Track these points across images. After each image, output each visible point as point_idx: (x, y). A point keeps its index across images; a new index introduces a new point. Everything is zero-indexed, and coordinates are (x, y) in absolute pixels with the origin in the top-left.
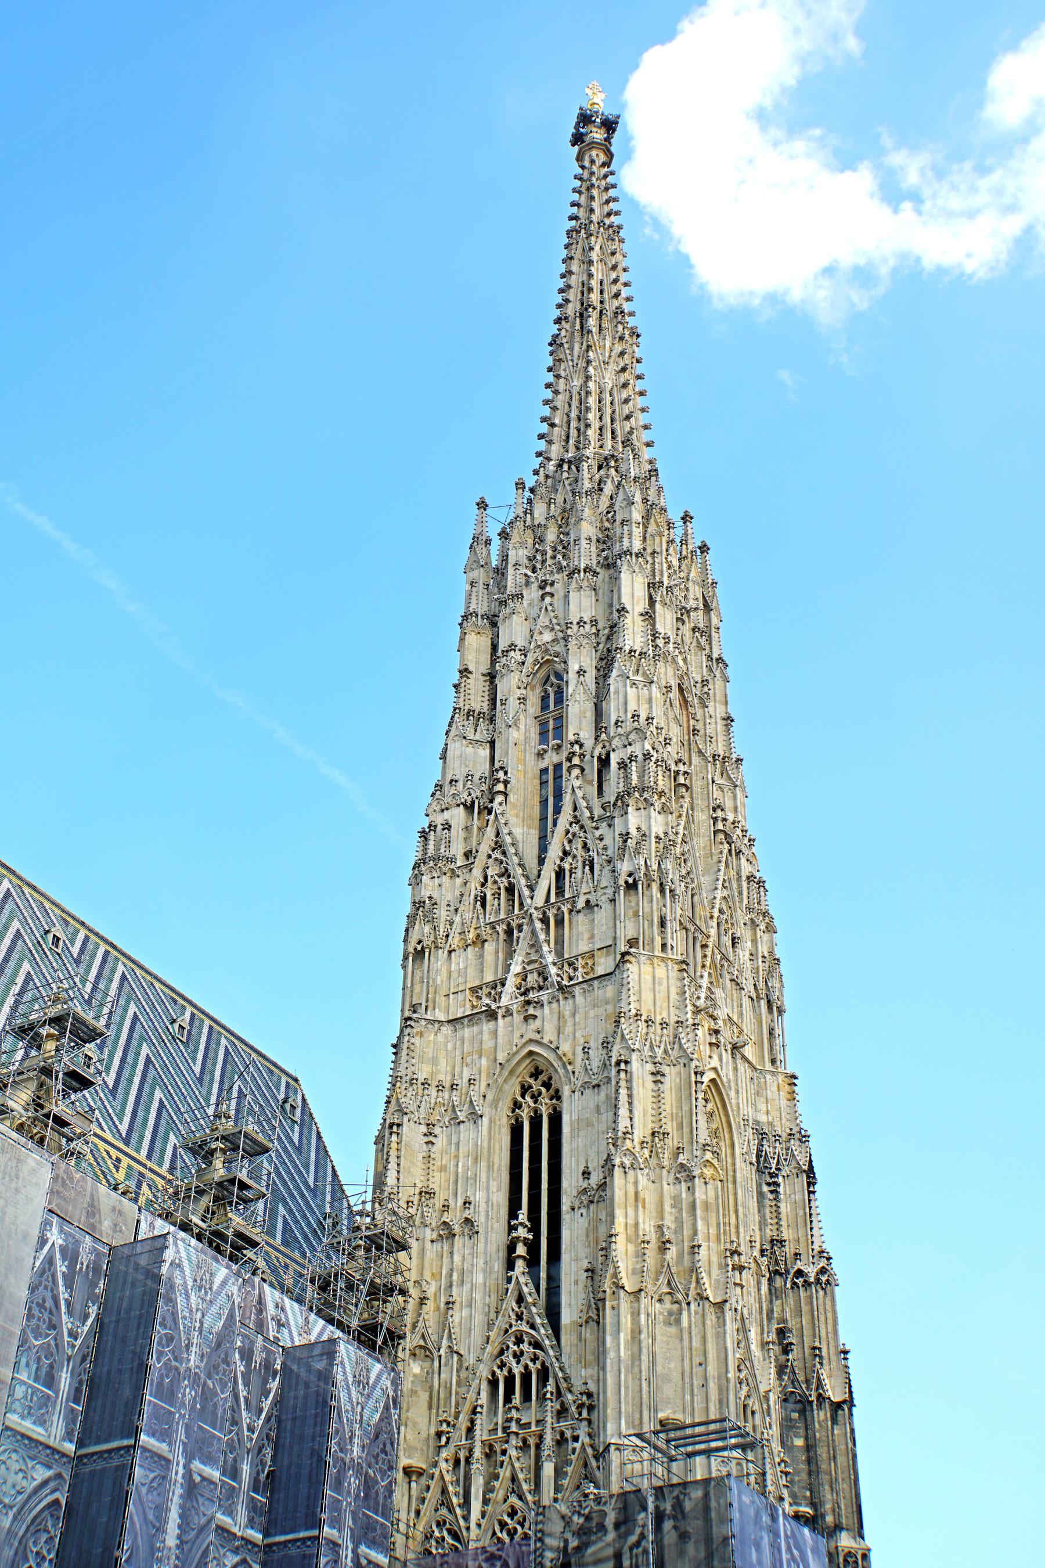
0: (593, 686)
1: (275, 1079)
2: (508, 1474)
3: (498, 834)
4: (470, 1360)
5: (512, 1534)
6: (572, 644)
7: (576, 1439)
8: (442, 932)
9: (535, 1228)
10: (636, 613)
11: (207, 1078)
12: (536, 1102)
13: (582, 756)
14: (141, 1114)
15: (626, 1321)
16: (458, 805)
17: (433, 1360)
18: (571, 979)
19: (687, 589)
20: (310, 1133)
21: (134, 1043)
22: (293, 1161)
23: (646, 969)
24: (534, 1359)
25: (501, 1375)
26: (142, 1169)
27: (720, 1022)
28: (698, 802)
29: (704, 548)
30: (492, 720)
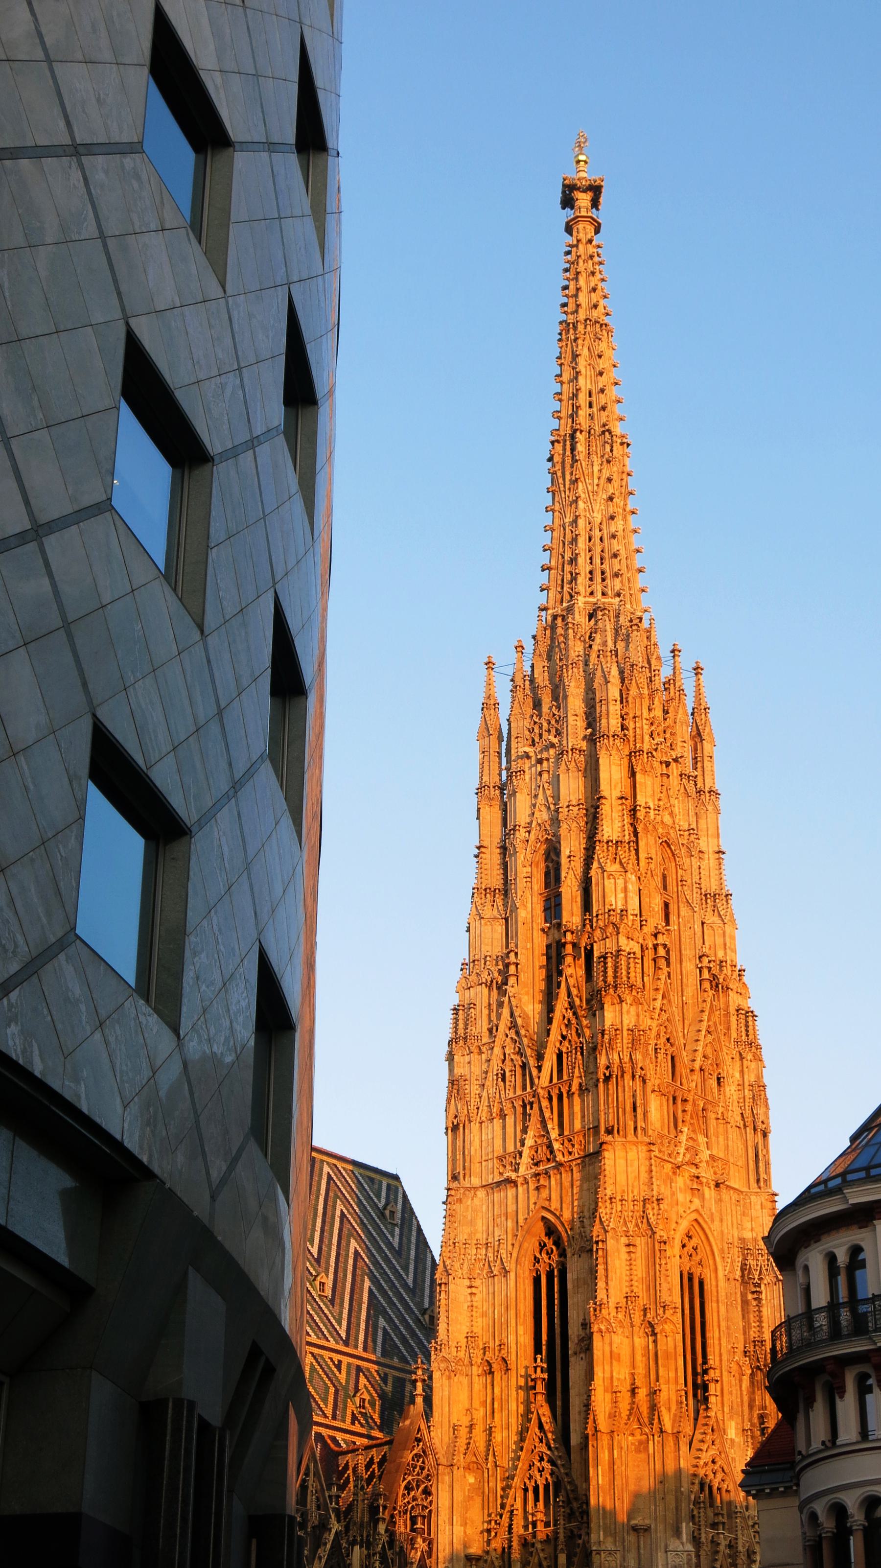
1: (376, 1186)
2: (536, 1560)
3: (512, 1014)
6: (563, 831)
8: (472, 1108)
10: (614, 798)
15: (604, 1456)
16: (481, 984)
18: (570, 1153)
20: (410, 1230)
23: (620, 1153)
25: (531, 1485)
27: (703, 1165)
28: (688, 952)
29: (698, 670)
30: (506, 893)
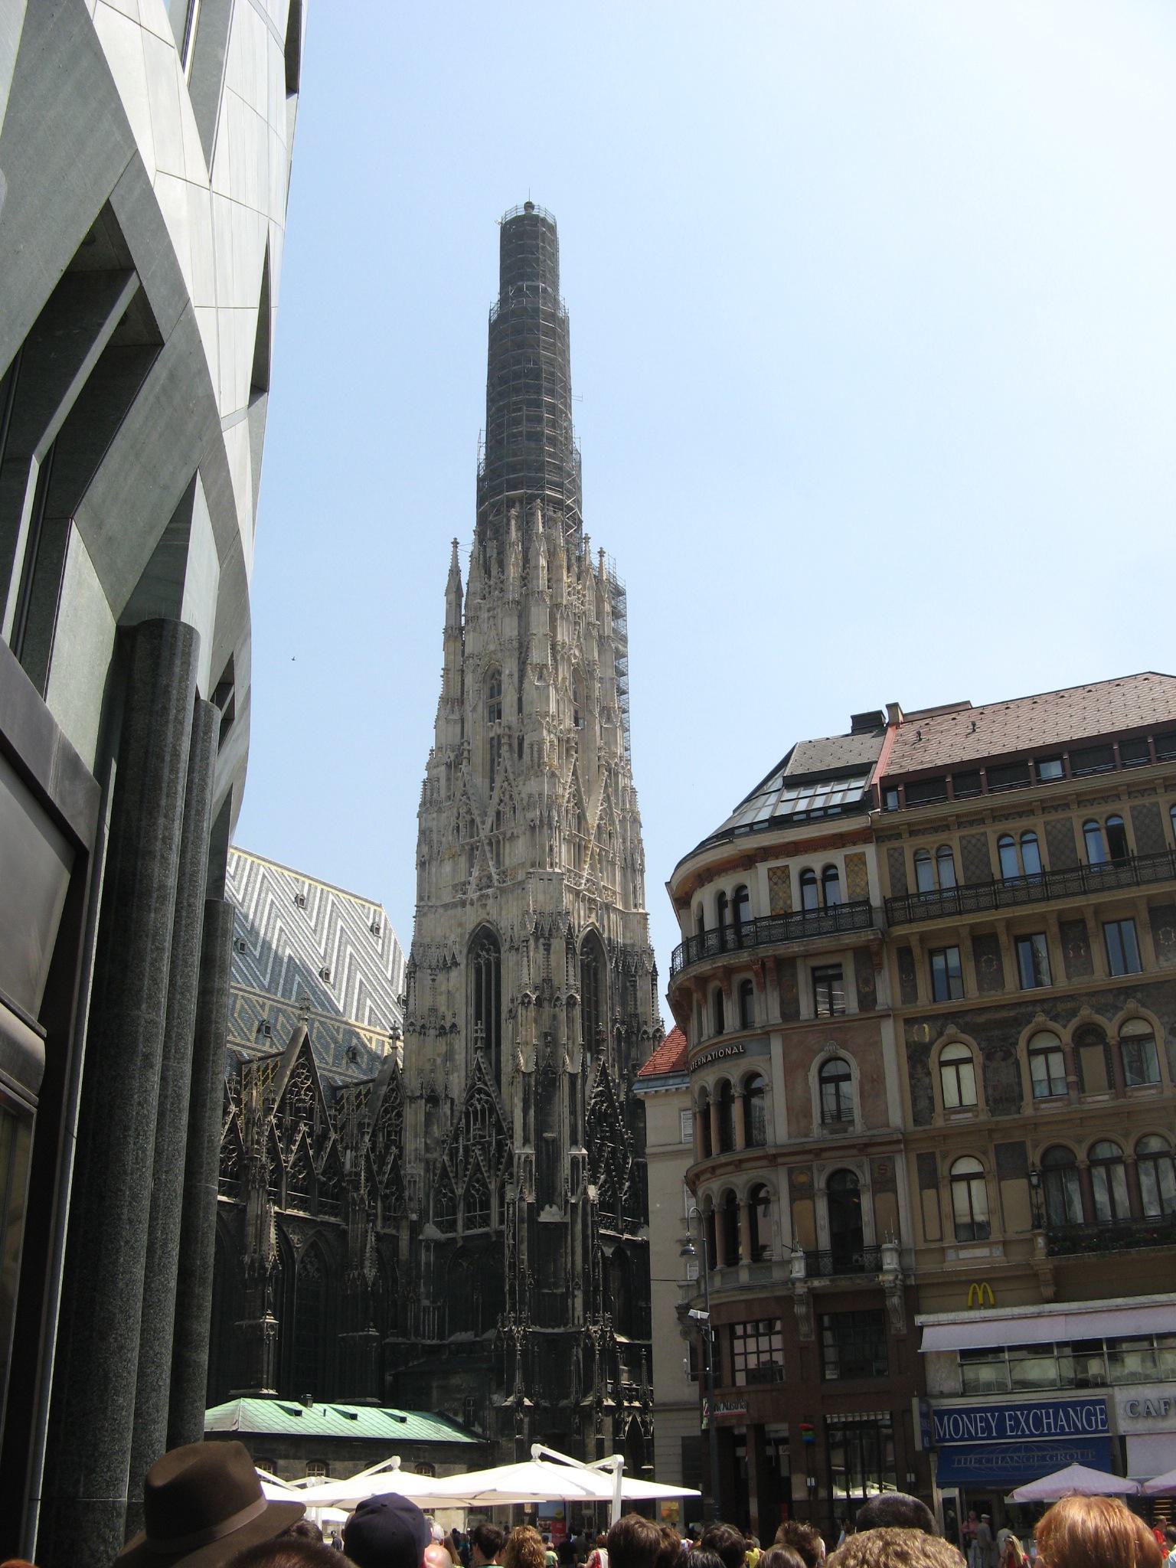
0: (516, 685)
1: (366, 911)
3: (465, 786)
4: (456, 1102)
5: (478, 1191)
7: (507, 1145)
8: (435, 851)
9: (488, 1030)
11: (320, 926)
12: (488, 954)
13: (510, 737)
14: (277, 969)
17: (438, 1101)
19: (584, 596)
20: (389, 942)
21: (272, 921)
22: (377, 965)
24: (487, 1102)
26: (279, 1005)
29: (601, 553)
30: (462, 703)
